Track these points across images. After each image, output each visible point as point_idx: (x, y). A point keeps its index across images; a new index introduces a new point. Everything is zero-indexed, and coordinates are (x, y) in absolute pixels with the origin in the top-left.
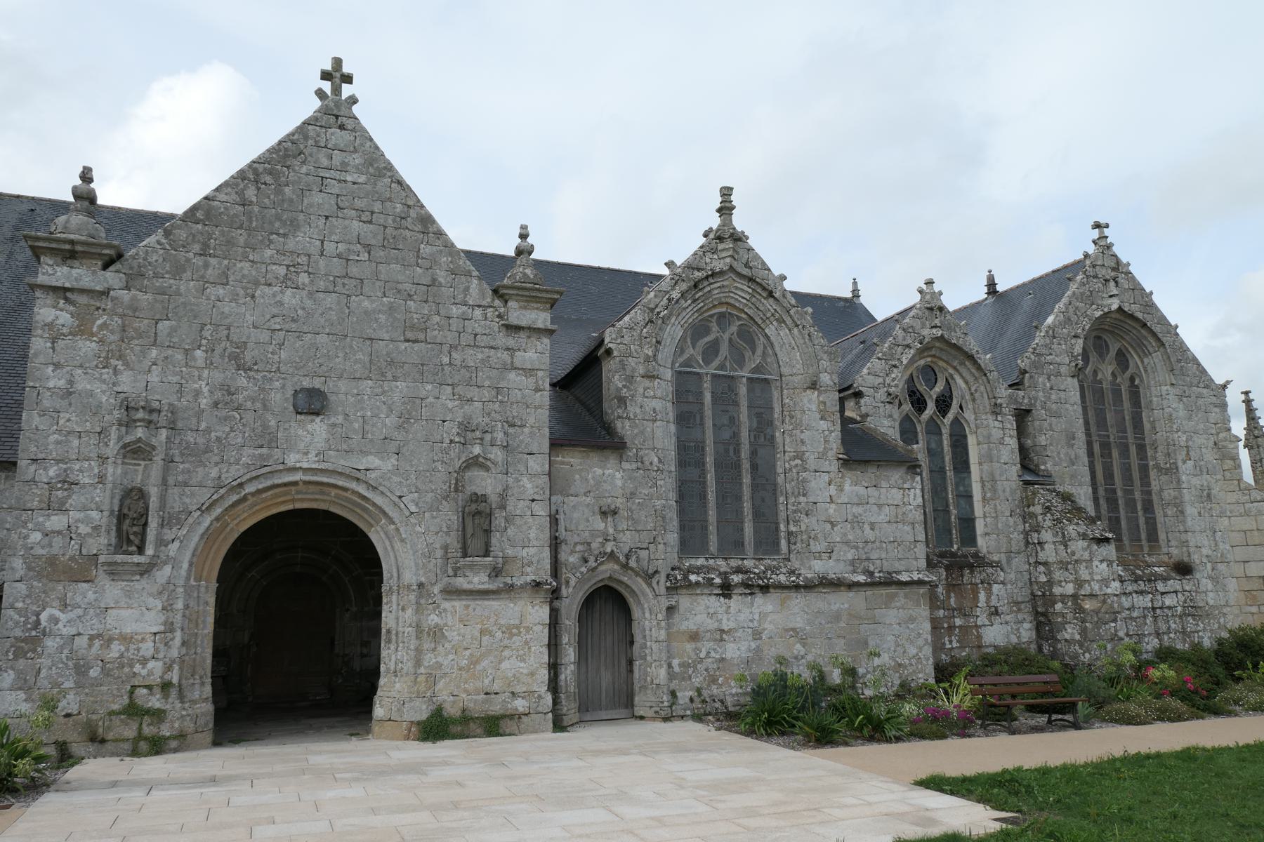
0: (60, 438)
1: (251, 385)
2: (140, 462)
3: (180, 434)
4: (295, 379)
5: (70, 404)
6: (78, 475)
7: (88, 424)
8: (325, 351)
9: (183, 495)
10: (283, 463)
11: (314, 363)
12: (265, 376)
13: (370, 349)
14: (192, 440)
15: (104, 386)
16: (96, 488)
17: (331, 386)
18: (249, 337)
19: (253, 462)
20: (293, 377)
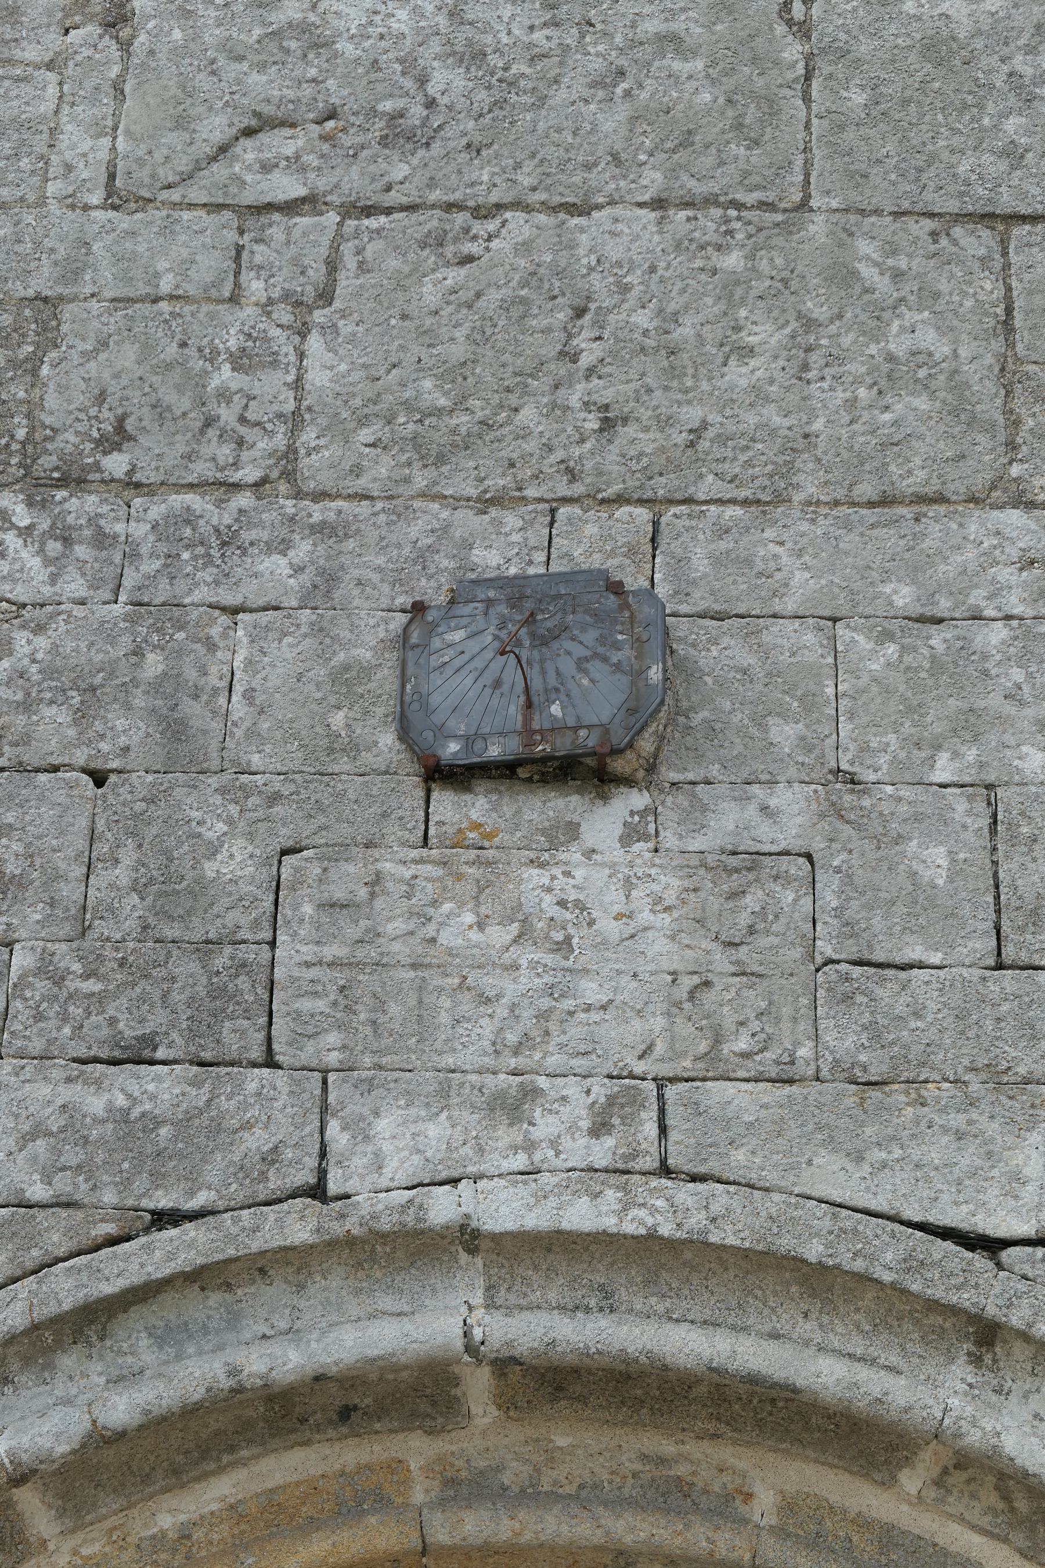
1: (74, 585)
4: (417, 530)
8: (643, 319)
10: (318, 1191)
11: (557, 410)
12: (189, 518)
13: (989, 287)
17: (700, 564)
18: (72, 272)
19: (63, 1184)
20: (400, 515)
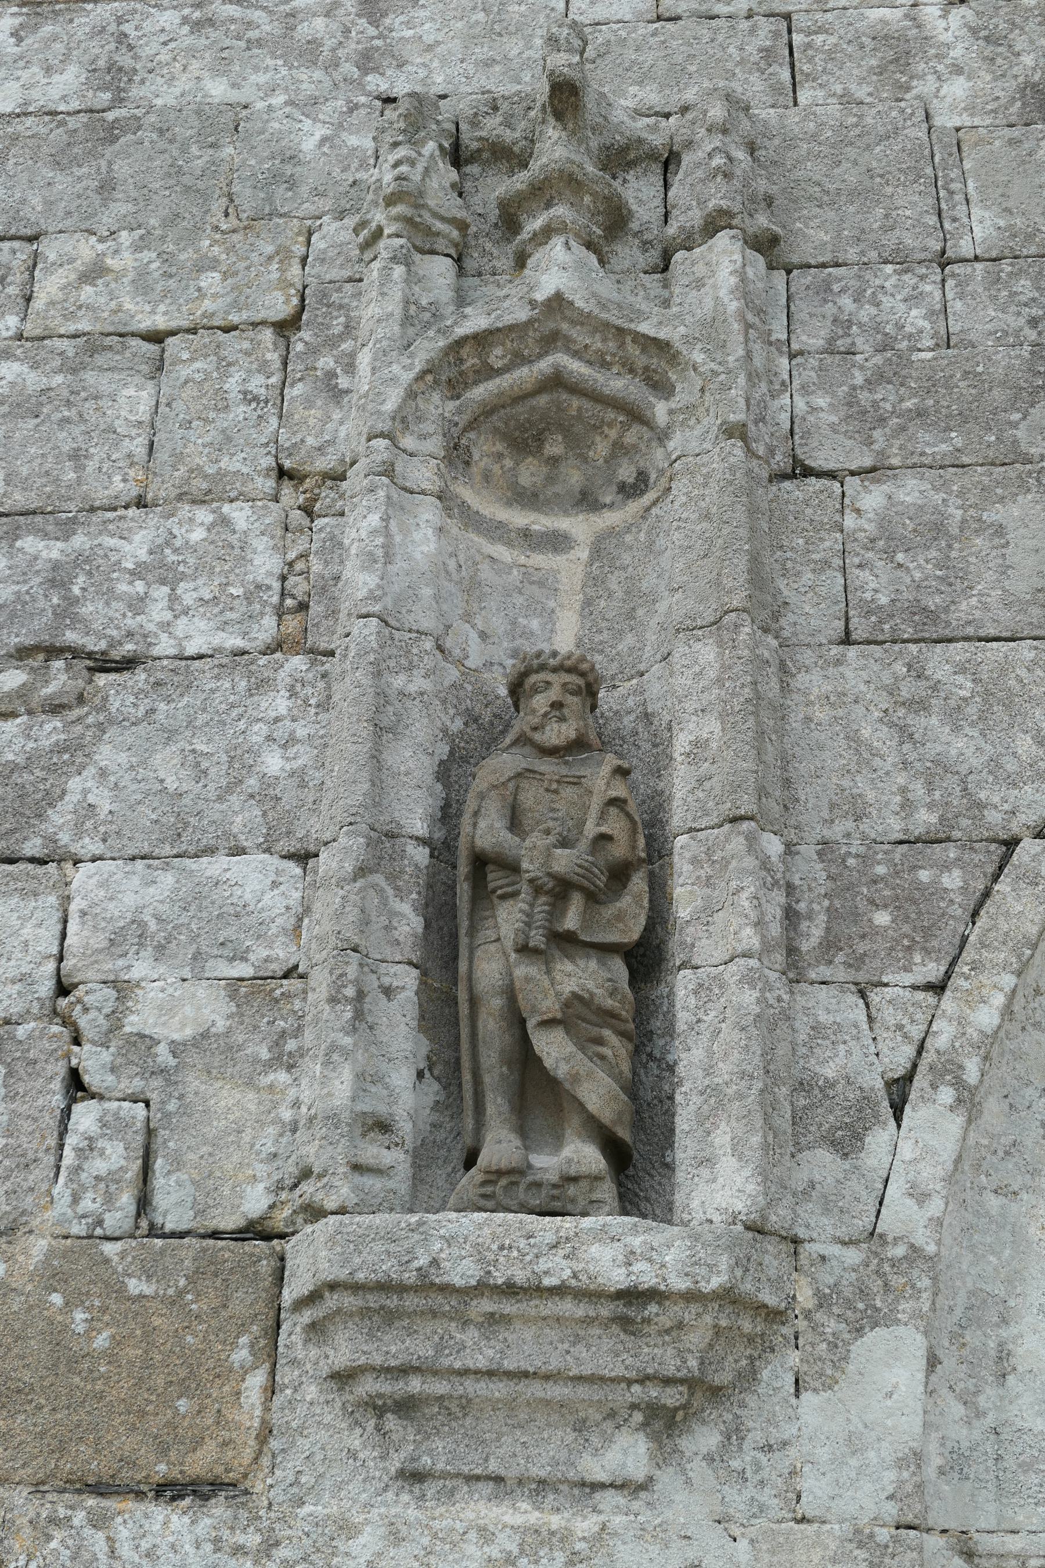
0: (34, 380)
2: (563, 523)
3: (825, 289)
5: (107, 187)
6: (138, 605)
7: (210, 280)
9: (917, 705)
14: (916, 318)
15: (303, 75)
16: (261, 685)
